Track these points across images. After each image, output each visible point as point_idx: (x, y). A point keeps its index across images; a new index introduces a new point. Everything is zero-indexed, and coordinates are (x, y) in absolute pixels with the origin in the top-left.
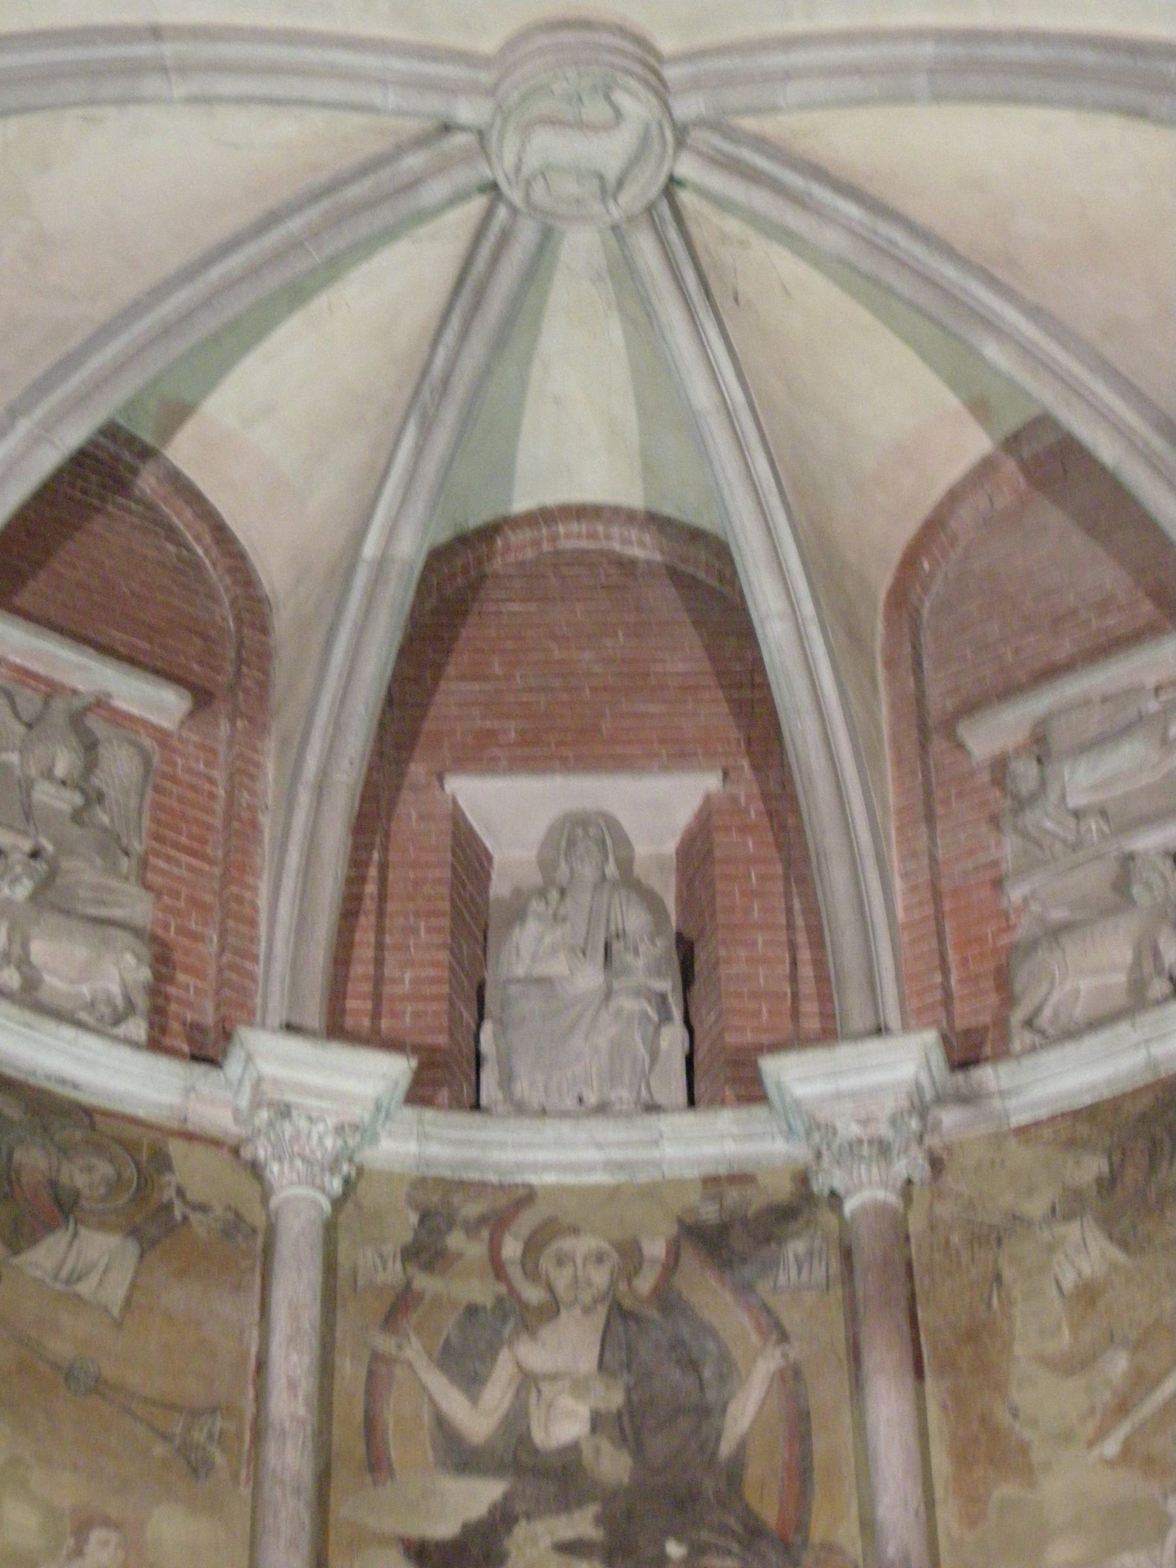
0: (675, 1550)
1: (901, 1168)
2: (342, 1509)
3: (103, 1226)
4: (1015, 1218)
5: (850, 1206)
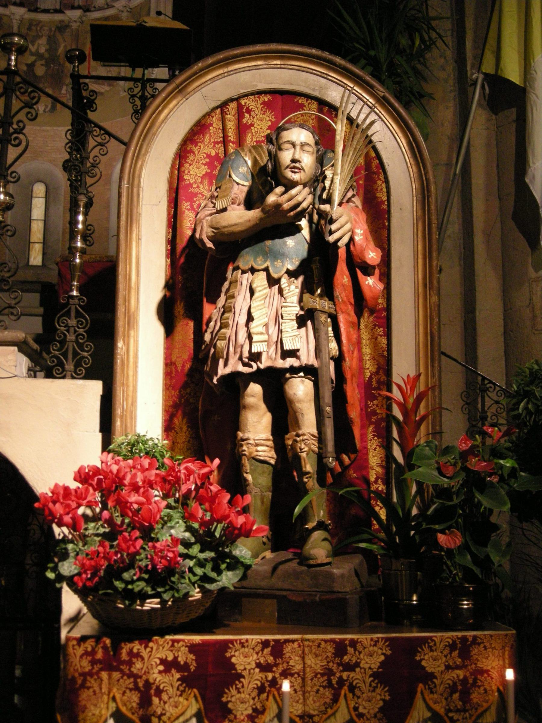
1: (79, 24)
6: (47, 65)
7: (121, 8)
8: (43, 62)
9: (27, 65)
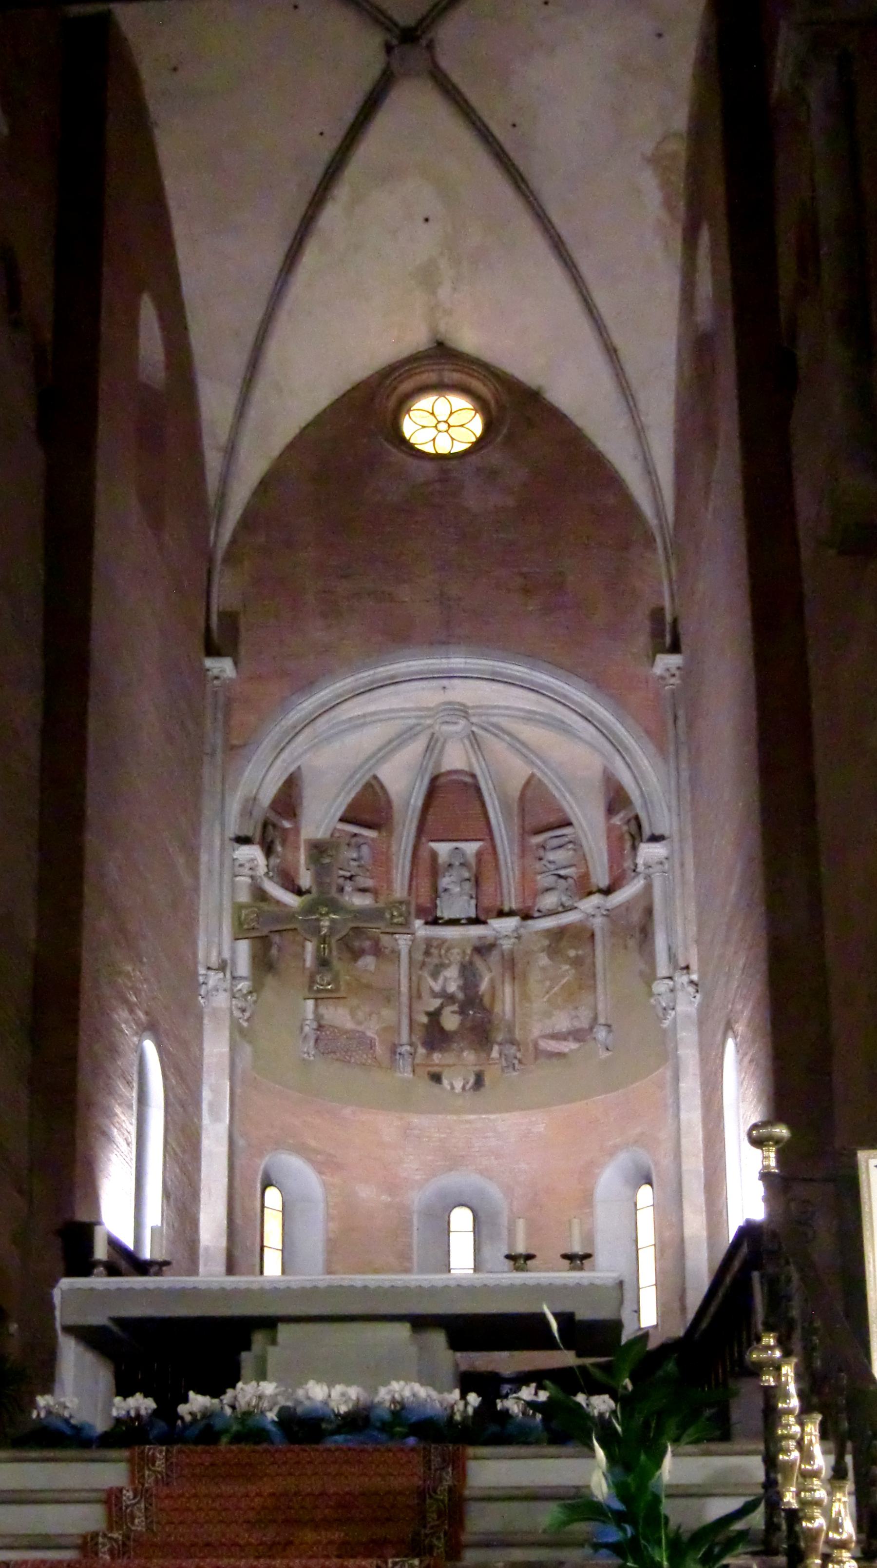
0: (471, 1012)
1: (513, 940)
2: (414, 1006)
3: (369, 954)
4: (533, 951)
5: (504, 947)
6: (462, 1012)
7: (591, 911)
8: (455, 1008)
9: (429, 1014)
